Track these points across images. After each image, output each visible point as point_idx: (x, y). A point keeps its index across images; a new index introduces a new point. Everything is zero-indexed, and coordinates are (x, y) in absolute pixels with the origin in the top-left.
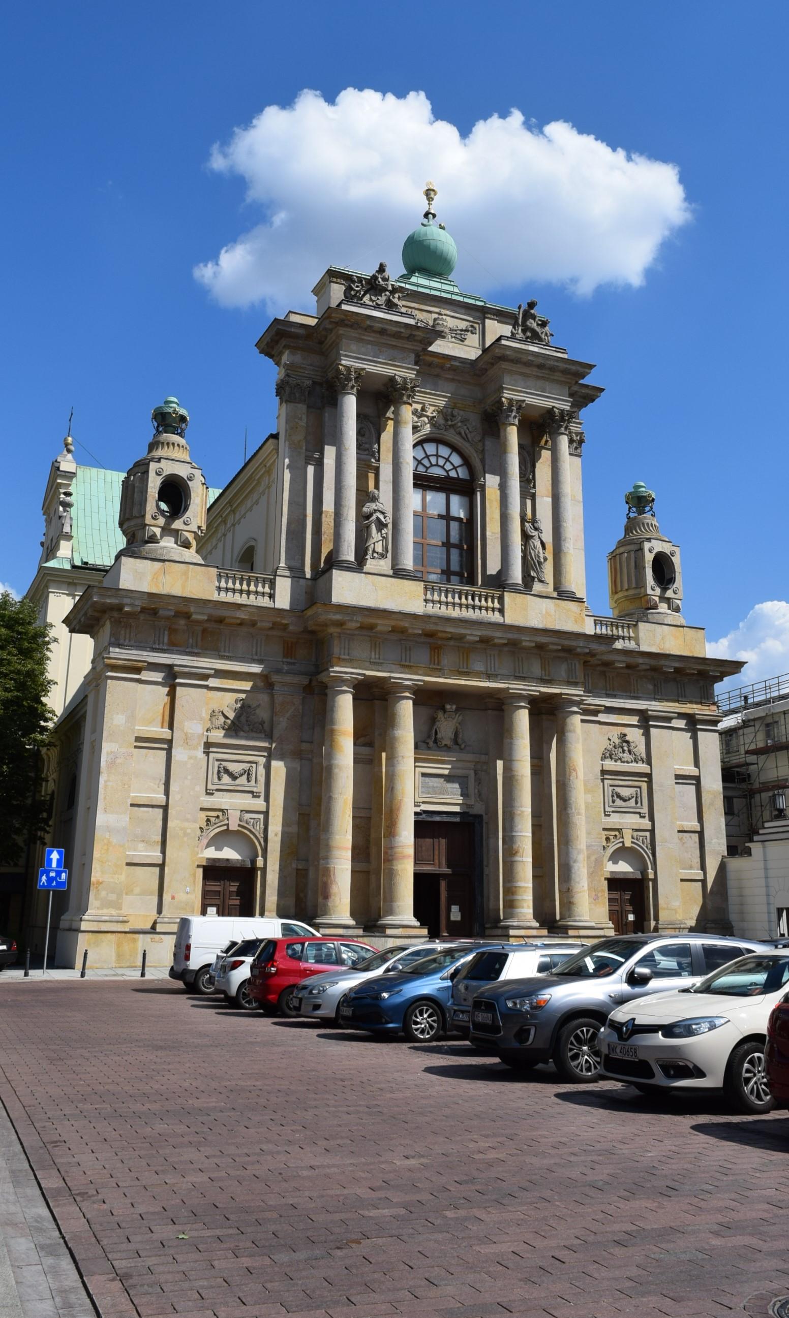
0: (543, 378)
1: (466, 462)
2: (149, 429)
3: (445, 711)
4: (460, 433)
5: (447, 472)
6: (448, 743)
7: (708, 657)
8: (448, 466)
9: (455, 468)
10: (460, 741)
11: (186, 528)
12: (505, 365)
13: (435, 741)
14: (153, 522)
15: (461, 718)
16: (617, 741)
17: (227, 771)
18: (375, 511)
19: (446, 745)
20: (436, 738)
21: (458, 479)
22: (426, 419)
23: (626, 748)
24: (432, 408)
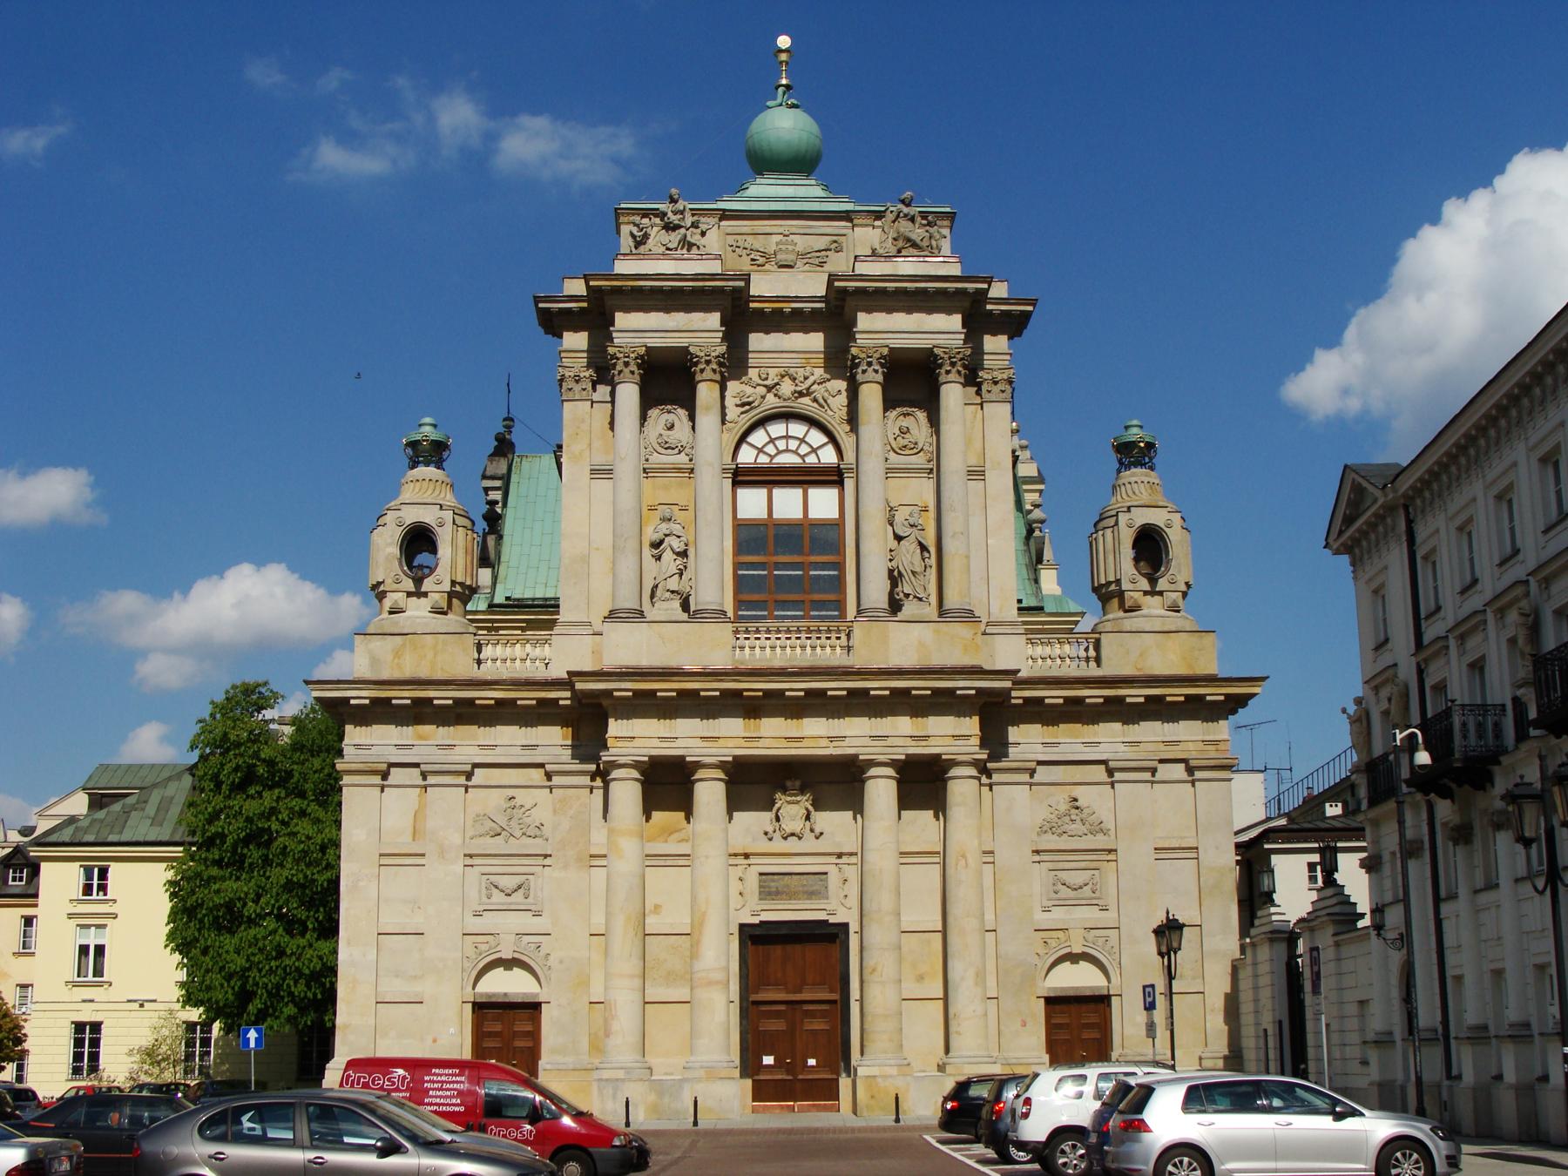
1: (833, 439)
4: (815, 400)
5: (802, 457)
8: (804, 449)
9: (814, 451)
11: (438, 588)
14: (395, 587)
16: (1063, 807)
17: (496, 887)
18: (666, 535)
19: (793, 835)
22: (763, 390)
23: (1073, 817)
24: (773, 372)
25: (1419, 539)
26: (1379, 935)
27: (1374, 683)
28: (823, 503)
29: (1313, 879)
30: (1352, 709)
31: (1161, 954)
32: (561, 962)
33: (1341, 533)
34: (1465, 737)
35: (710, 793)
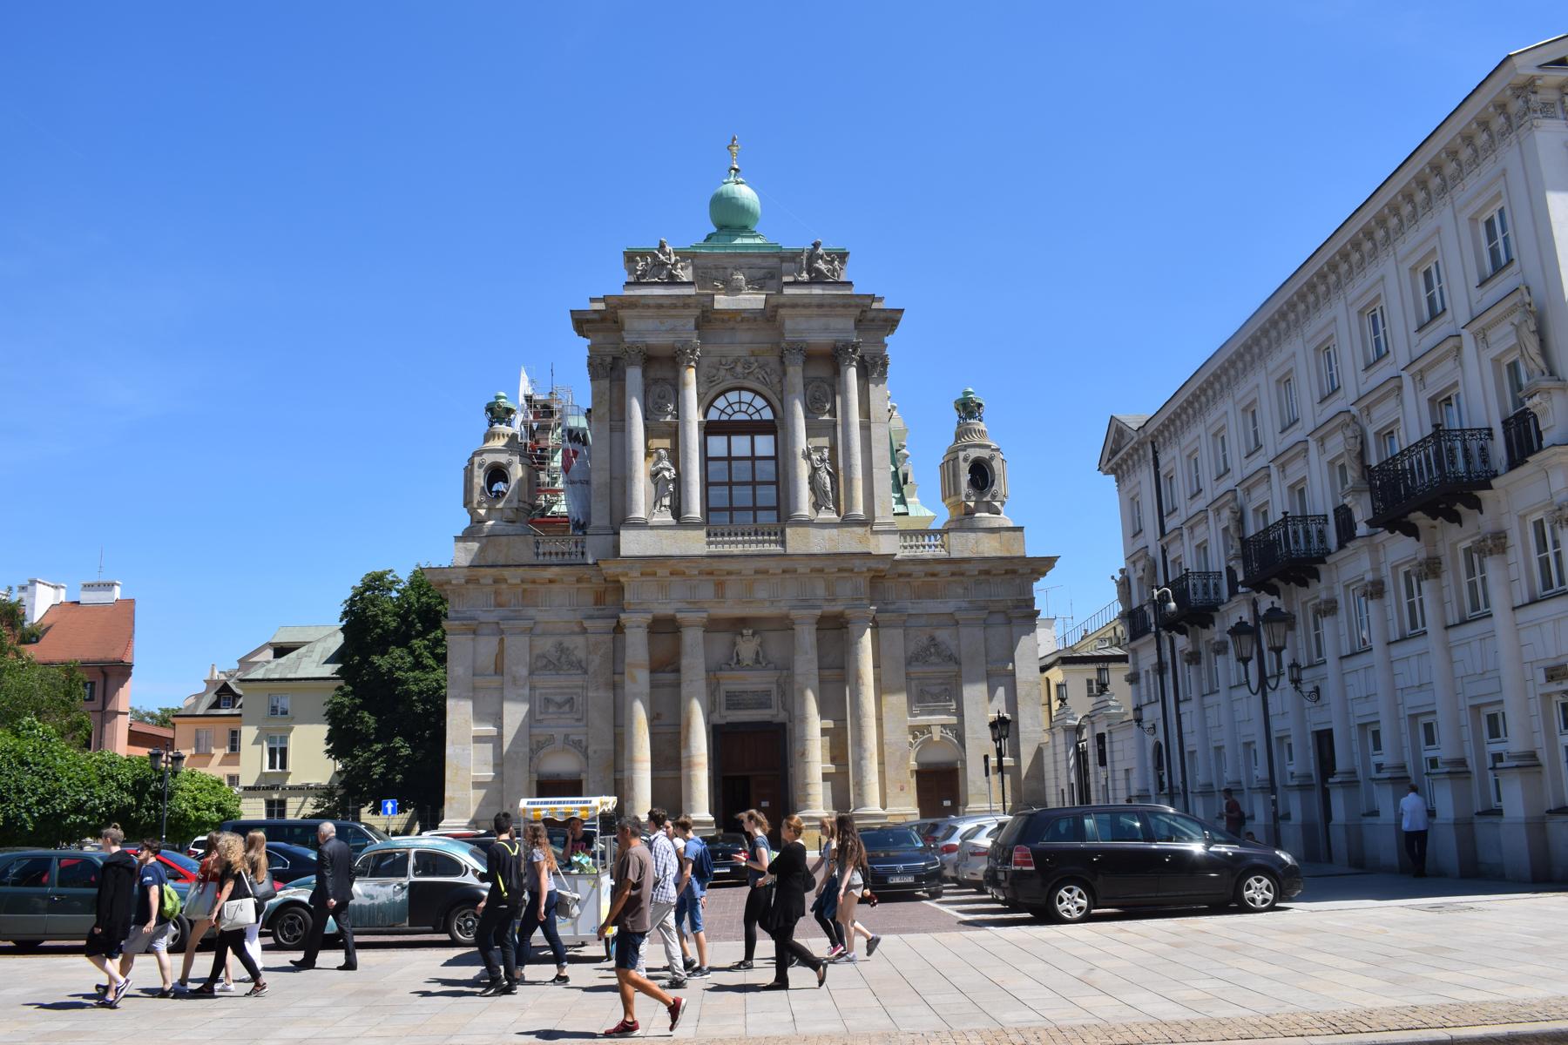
0: (825, 316)
1: (770, 404)
2: (483, 421)
3: (742, 635)
5: (750, 416)
6: (750, 663)
7: (1029, 555)
8: (751, 410)
9: (758, 411)
10: (761, 659)
12: (782, 311)
13: (738, 660)
15: (759, 641)
20: (738, 660)
21: (762, 421)
22: (722, 373)
25: (1161, 463)
26: (1139, 725)
27: (1133, 559)
28: (764, 445)
29: (1090, 690)
30: (1118, 576)
31: (995, 740)
32: (595, 752)
33: (1109, 460)
34: (1195, 594)
35: (693, 639)
